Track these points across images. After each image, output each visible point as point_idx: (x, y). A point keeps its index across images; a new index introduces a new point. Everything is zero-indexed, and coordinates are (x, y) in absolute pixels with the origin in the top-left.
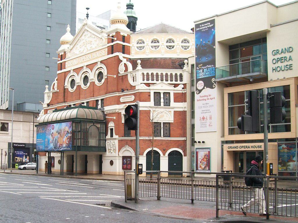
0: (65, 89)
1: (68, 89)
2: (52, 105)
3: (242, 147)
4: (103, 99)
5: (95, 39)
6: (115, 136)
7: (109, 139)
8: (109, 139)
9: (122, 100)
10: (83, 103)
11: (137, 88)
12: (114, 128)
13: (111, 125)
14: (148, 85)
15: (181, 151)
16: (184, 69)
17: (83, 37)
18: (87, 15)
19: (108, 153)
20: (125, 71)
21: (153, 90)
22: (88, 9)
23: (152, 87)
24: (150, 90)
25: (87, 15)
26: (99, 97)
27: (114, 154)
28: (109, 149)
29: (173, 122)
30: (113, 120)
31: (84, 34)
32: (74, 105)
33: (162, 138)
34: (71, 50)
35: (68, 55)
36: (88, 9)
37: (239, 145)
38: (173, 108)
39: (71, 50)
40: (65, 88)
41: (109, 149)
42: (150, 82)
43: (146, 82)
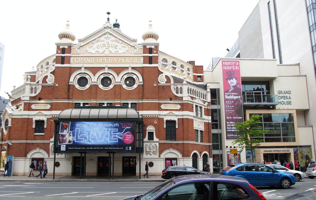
0: (69, 85)
1: (74, 86)
2: (42, 99)
3: (275, 151)
4: (136, 103)
5: (123, 45)
6: (155, 139)
7: (146, 142)
8: (146, 142)
9: (163, 107)
10: (104, 104)
11: (184, 99)
12: (154, 132)
13: (150, 128)
14: (192, 98)
15: (208, 154)
16: (207, 91)
17: (103, 38)
18: (108, 19)
19: (145, 156)
20: (166, 82)
21: (195, 103)
22: (109, 13)
23: (194, 101)
24: (193, 102)
25: (108, 19)
26: (129, 101)
27: (153, 156)
28: (146, 152)
29: (203, 130)
30: (154, 125)
31: (107, 35)
32: (84, 104)
33: (199, 143)
34: (80, 47)
35: (74, 51)
36: (109, 13)
37: (273, 149)
38: (204, 119)
39: (80, 47)
40: (70, 84)
41: (146, 152)
42: (194, 96)
43: (190, 95)
